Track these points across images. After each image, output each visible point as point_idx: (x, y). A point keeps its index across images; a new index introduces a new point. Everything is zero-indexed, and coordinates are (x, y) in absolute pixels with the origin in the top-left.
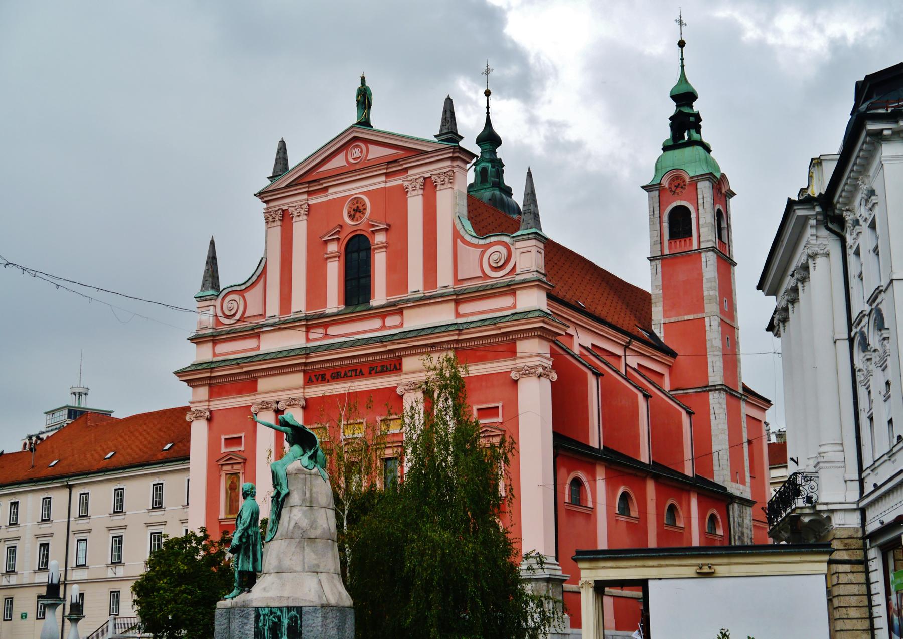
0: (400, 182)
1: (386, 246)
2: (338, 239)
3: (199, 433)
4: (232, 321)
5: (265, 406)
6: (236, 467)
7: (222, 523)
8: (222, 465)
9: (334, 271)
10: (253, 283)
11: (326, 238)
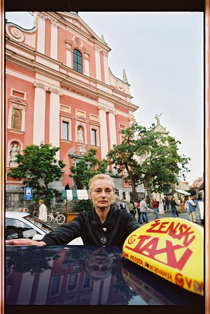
0: (94, 46)
5: (42, 87)
6: (20, 106)
7: (9, 131)
8: (12, 102)
10: (29, 33)
11: (68, 42)
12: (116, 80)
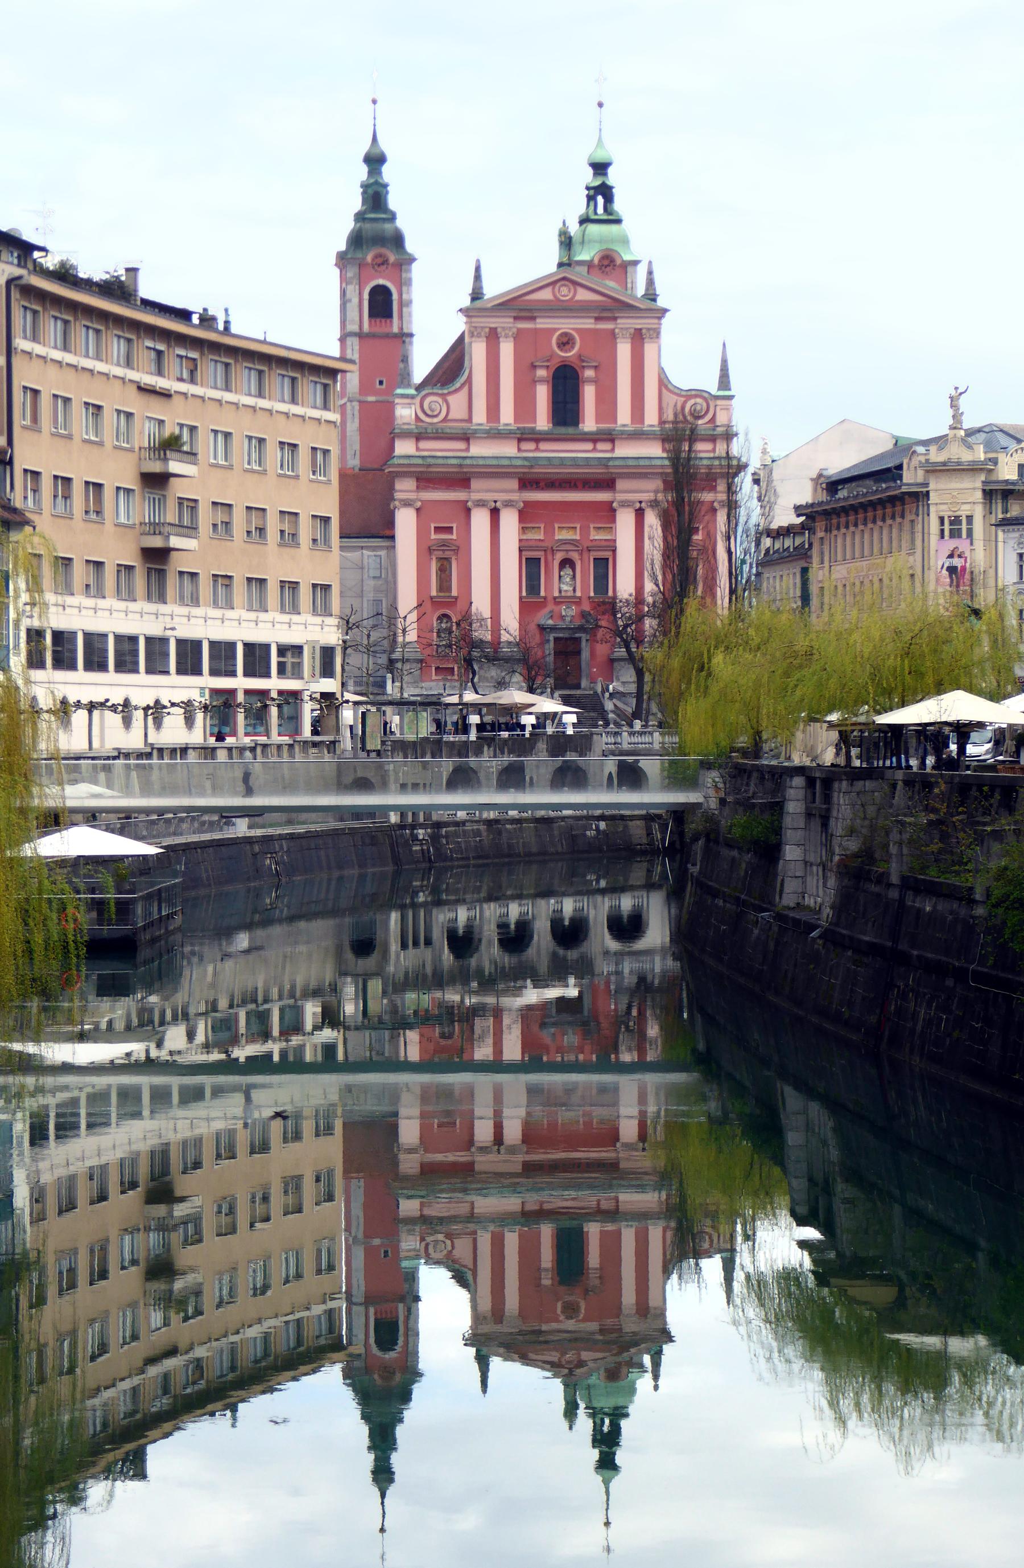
1: (595, 381)
2: (548, 367)
3: (406, 522)
4: (435, 420)
5: (481, 504)
6: (447, 553)
9: (543, 394)
12: (682, 396)
